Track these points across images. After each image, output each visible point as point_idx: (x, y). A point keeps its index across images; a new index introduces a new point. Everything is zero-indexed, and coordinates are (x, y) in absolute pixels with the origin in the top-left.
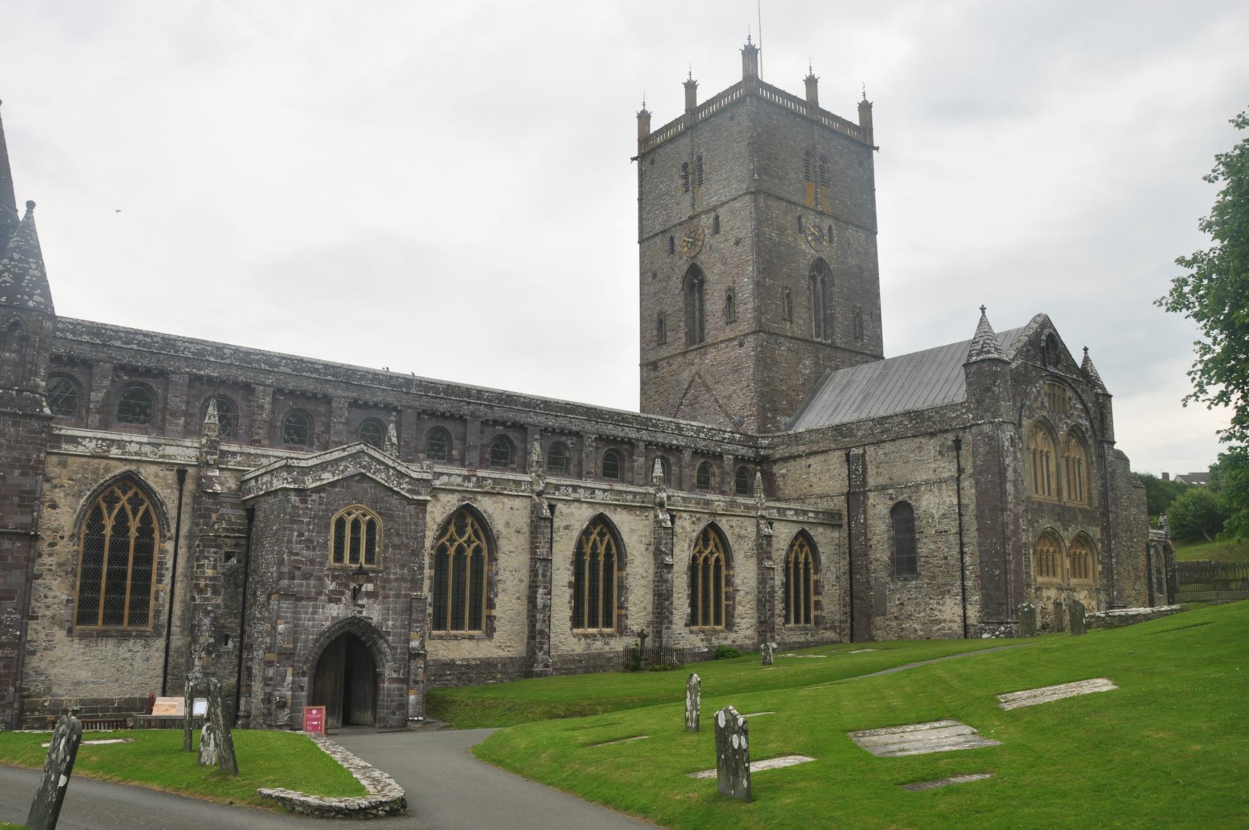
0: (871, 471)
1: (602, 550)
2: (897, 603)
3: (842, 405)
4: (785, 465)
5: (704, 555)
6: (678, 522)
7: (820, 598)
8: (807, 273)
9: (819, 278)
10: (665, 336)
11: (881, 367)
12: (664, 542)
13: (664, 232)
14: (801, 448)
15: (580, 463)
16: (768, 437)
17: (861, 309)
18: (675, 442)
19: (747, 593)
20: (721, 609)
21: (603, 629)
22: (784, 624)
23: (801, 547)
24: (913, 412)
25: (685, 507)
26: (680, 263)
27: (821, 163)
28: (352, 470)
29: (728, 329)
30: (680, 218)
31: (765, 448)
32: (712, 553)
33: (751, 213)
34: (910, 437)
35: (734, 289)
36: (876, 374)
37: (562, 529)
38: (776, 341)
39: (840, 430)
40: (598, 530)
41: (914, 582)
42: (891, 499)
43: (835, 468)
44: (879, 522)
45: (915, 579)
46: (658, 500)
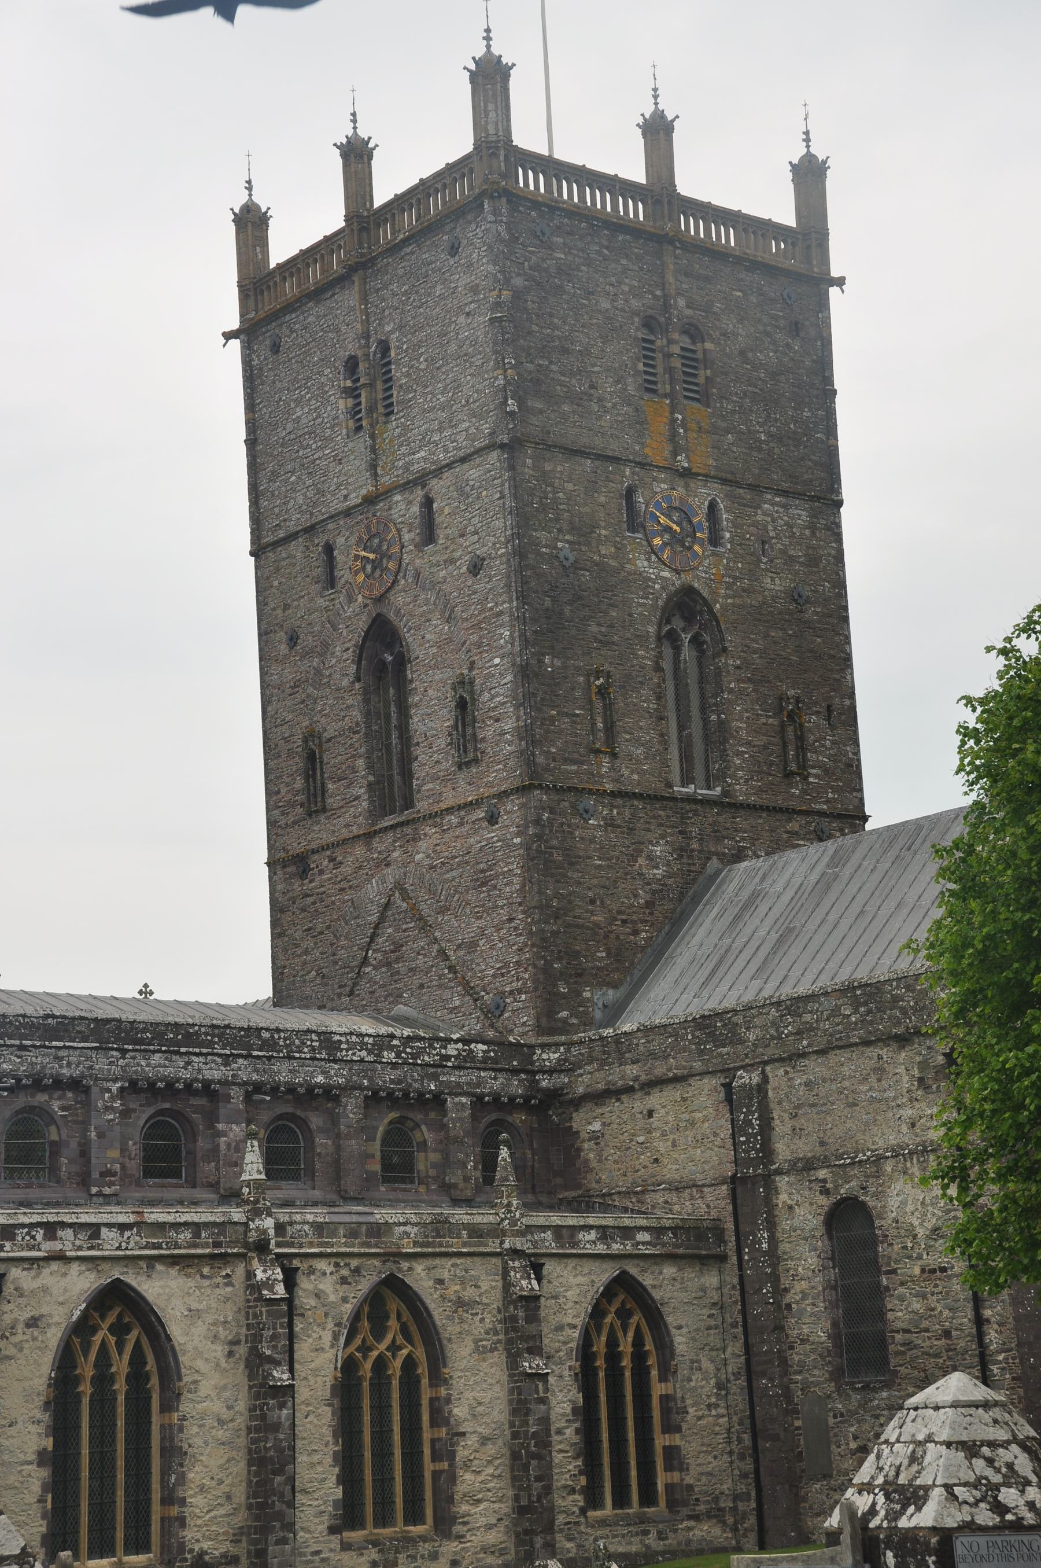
0: (781, 1126)
1: (121, 1366)
2: (853, 1445)
3: (731, 957)
4: (599, 1111)
5: (375, 1354)
6: (305, 1284)
7: (677, 1440)
8: (652, 630)
9: (686, 638)
10: (324, 791)
11: (826, 859)
12: (267, 1333)
13: (310, 530)
14: (632, 1070)
15: (84, 1153)
16: (558, 1045)
17: (798, 700)
18: (320, 1079)
19: (484, 1440)
20: (422, 1484)
21: (126, 1559)
22: (583, 1511)
23: (624, 1315)
24: (860, 986)
25: (321, 1245)
26: (349, 612)
27: (686, 342)
29: (462, 778)
30: (346, 497)
31: (551, 1072)
32: (394, 1348)
33: (502, 497)
34: (856, 1044)
35: (472, 683)
36: (814, 878)
37: (20, 1328)
38: (573, 806)
40: (111, 1318)
41: (884, 1394)
42: (825, 1192)
43: (706, 1119)
44: (804, 1248)
45: (888, 1385)
46: (253, 1236)
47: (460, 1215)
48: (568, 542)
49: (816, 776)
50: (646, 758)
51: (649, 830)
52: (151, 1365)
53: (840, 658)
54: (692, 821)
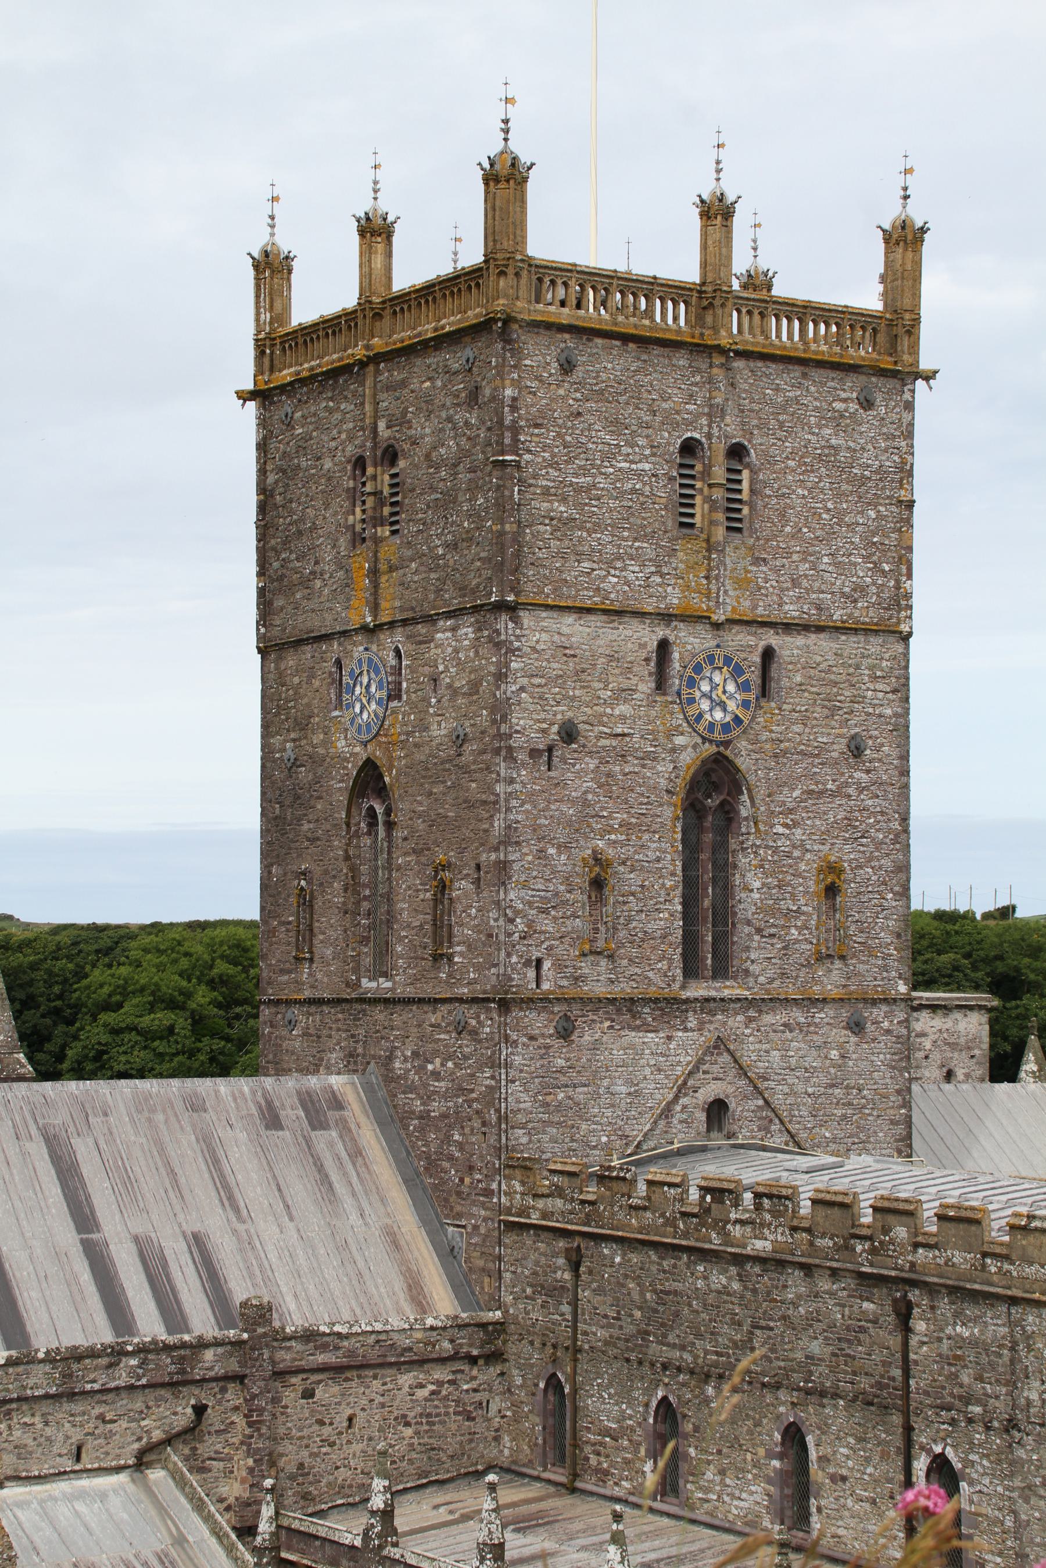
48: (294, 740)
49: (461, 954)
50: (333, 959)
51: (330, 1036)
53: (490, 803)
54: (361, 1022)
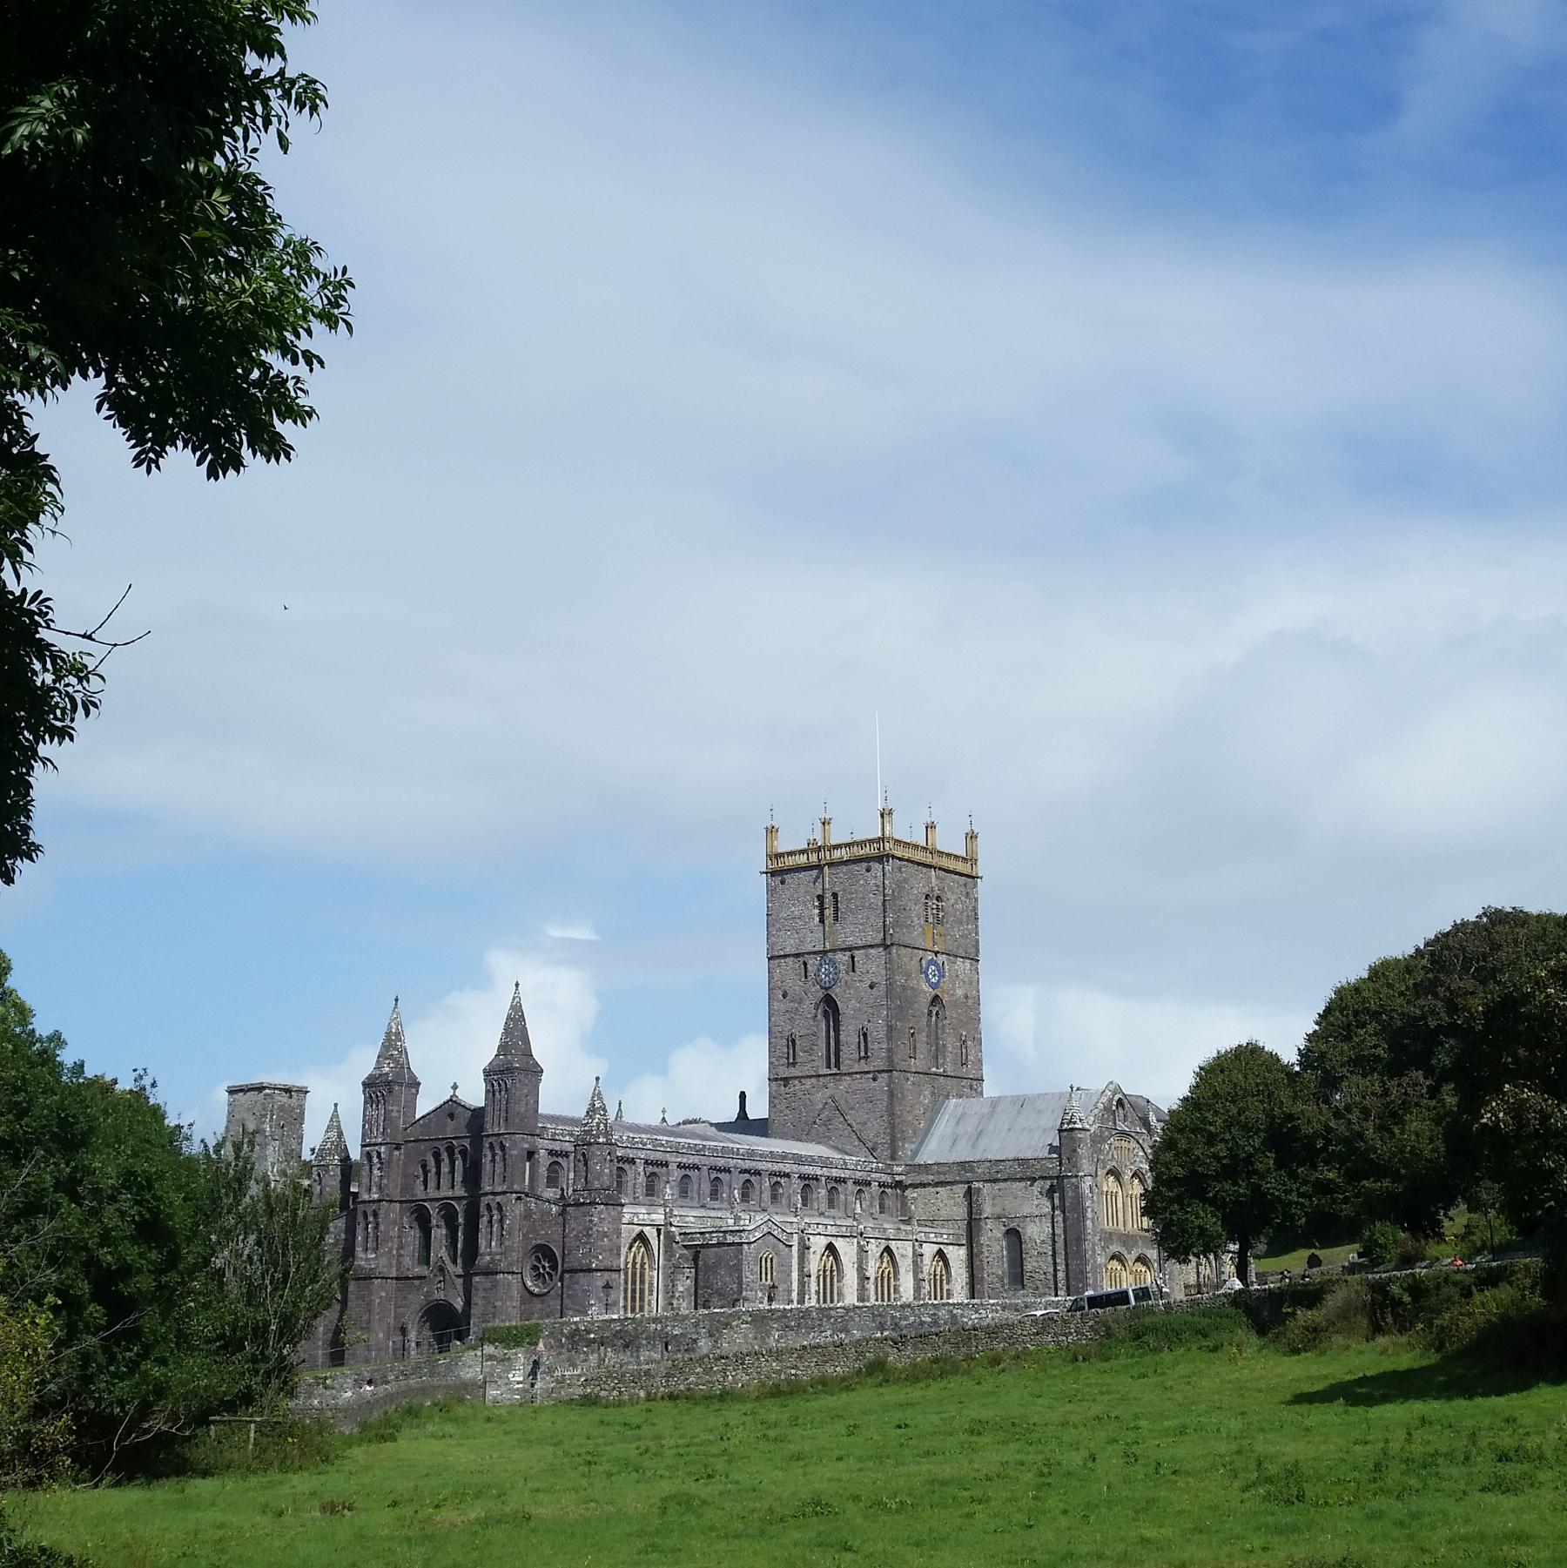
1: (828, 1267)
13: (797, 955)
28: (766, 1230)
39: (964, 1165)
42: (1005, 1226)
45: (1023, 1288)
47: (903, 1227)
52: (834, 1268)
